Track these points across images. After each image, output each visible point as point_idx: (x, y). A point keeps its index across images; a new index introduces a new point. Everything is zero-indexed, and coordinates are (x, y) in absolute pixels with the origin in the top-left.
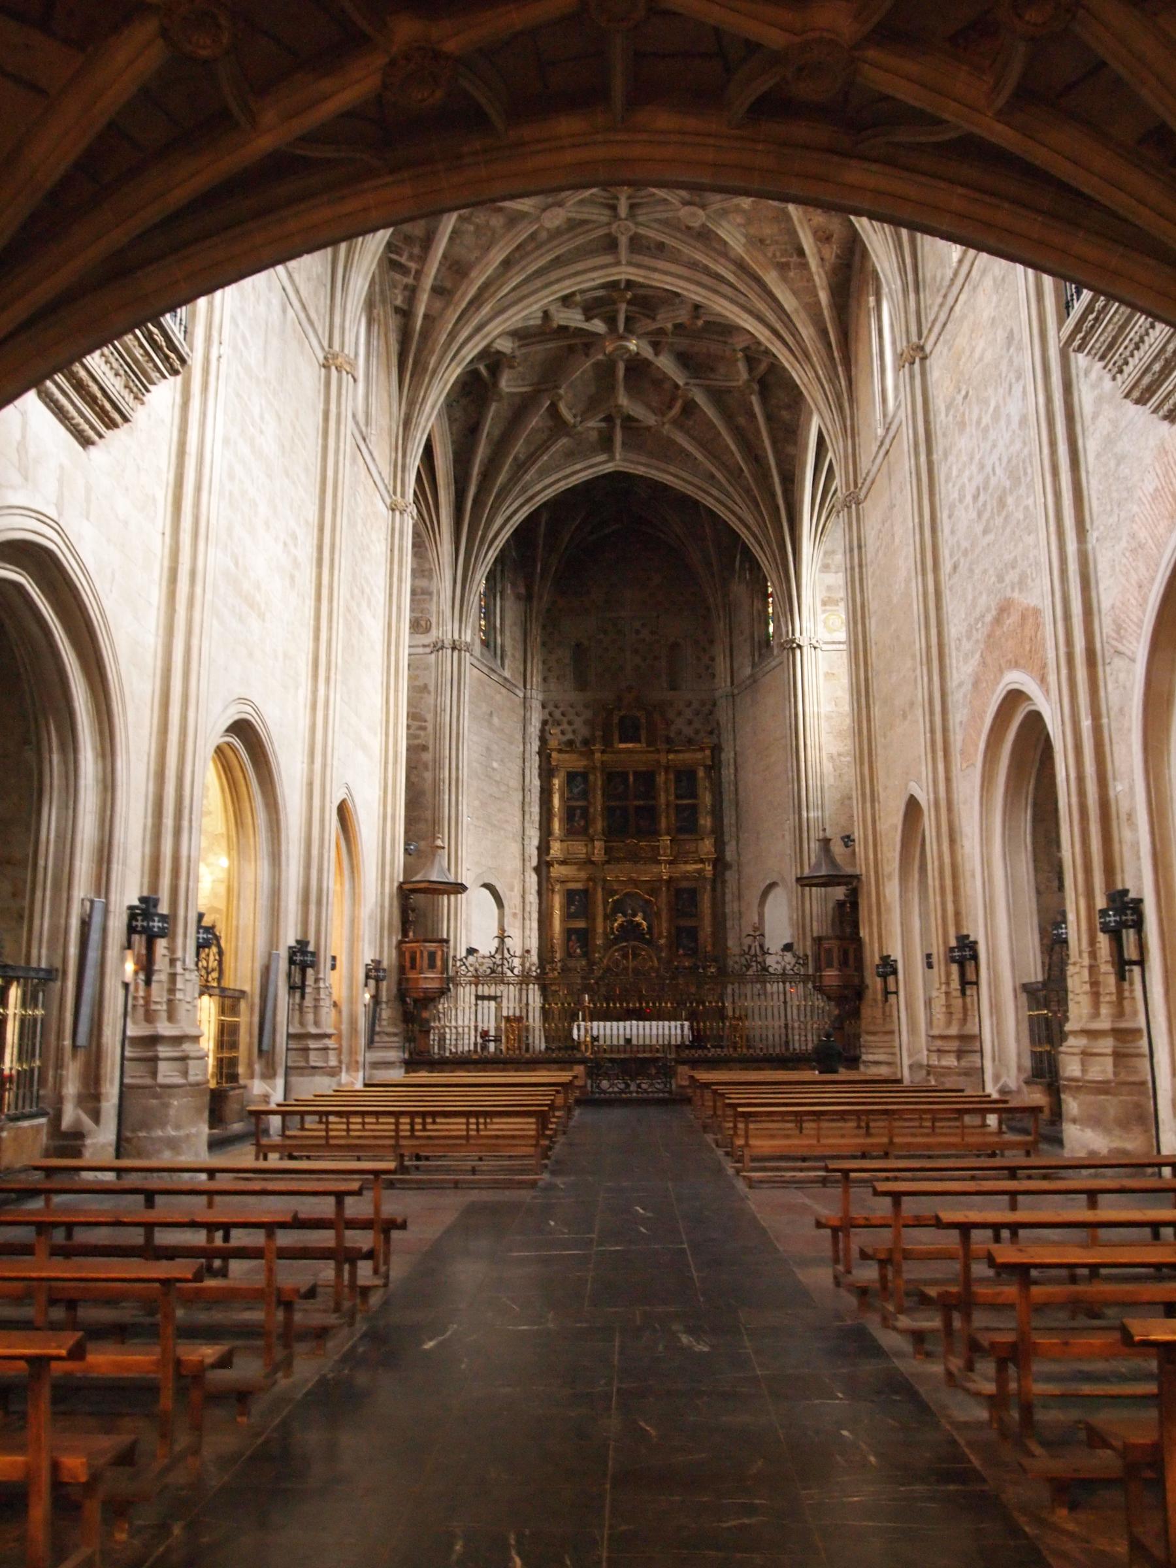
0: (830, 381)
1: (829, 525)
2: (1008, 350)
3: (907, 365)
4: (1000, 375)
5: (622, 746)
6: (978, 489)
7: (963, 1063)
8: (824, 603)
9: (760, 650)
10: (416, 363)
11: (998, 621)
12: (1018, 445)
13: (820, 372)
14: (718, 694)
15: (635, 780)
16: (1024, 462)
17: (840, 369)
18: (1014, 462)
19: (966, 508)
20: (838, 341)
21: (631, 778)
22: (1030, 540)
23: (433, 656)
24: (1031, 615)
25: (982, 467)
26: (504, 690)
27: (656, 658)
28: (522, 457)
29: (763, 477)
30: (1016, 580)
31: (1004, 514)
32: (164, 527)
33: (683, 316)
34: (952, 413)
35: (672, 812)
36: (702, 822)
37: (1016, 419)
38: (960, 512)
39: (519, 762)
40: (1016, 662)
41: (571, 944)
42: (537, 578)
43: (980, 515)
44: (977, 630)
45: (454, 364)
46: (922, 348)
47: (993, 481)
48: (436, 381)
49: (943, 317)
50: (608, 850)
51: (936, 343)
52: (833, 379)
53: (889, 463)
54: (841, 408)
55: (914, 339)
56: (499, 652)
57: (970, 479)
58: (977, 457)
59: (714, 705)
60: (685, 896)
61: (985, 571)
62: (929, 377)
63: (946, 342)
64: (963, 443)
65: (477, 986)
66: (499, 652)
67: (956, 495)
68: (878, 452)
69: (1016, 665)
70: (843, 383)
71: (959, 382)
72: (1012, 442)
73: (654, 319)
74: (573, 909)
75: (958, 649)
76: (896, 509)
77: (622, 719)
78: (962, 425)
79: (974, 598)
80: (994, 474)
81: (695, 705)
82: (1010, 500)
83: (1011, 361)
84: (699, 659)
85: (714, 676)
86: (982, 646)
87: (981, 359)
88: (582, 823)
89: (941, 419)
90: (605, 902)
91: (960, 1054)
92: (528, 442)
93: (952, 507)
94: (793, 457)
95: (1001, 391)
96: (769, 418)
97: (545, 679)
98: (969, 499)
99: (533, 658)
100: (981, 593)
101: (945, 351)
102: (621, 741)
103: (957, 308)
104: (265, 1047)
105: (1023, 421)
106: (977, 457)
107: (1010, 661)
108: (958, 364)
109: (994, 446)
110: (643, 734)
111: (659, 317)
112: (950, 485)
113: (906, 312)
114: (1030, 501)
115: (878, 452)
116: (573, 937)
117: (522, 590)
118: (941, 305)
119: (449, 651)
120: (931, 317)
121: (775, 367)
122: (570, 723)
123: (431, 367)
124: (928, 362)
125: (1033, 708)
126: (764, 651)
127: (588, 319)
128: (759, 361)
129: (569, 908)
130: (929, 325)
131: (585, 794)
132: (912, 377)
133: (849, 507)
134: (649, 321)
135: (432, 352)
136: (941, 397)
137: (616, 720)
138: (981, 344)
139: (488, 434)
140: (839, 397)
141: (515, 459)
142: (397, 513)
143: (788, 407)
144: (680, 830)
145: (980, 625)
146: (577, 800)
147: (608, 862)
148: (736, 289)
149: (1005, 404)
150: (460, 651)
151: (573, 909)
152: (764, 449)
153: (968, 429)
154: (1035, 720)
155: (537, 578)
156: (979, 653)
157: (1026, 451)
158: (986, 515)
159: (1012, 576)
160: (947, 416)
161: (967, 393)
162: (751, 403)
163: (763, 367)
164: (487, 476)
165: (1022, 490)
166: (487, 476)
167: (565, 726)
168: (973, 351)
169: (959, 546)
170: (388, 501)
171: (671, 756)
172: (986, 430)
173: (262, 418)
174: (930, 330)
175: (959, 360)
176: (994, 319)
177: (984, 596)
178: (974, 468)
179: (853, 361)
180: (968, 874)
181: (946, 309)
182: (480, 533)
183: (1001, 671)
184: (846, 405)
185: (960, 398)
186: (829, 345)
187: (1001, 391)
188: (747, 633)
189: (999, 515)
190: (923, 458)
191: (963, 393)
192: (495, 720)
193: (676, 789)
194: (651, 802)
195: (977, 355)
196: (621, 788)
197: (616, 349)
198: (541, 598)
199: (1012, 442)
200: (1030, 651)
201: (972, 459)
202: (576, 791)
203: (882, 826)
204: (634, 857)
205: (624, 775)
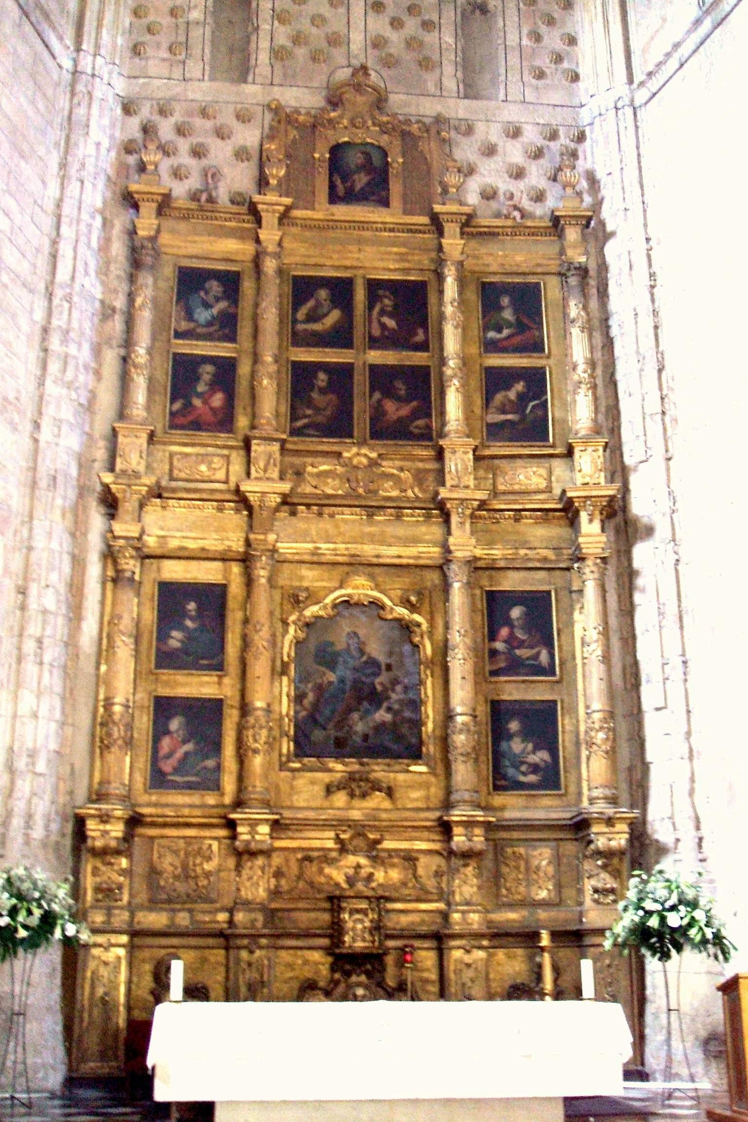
14: (585, 117)
27: (427, 25)
35: (476, 382)
39: (48, 223)
41: (166, 743)
59: (581, 138)
60: (516, 613)
74: (176, 638)
77: (336, 150)
81: (531, 136)
84: (537, 37)
85: (575, 78)
88: (218, 400)
97: (136, 50)
102: (334, 198)
110: (396, 188)
122: (198, 152)
129: (162, 635)
137: (322, 154)
144: (495, 431)
146: (209, 337)
147: (288, 502)
151: (176, 638)
167: (184, 158)
193: (486, 328)
194: (418, 358)
202: (203, 315)
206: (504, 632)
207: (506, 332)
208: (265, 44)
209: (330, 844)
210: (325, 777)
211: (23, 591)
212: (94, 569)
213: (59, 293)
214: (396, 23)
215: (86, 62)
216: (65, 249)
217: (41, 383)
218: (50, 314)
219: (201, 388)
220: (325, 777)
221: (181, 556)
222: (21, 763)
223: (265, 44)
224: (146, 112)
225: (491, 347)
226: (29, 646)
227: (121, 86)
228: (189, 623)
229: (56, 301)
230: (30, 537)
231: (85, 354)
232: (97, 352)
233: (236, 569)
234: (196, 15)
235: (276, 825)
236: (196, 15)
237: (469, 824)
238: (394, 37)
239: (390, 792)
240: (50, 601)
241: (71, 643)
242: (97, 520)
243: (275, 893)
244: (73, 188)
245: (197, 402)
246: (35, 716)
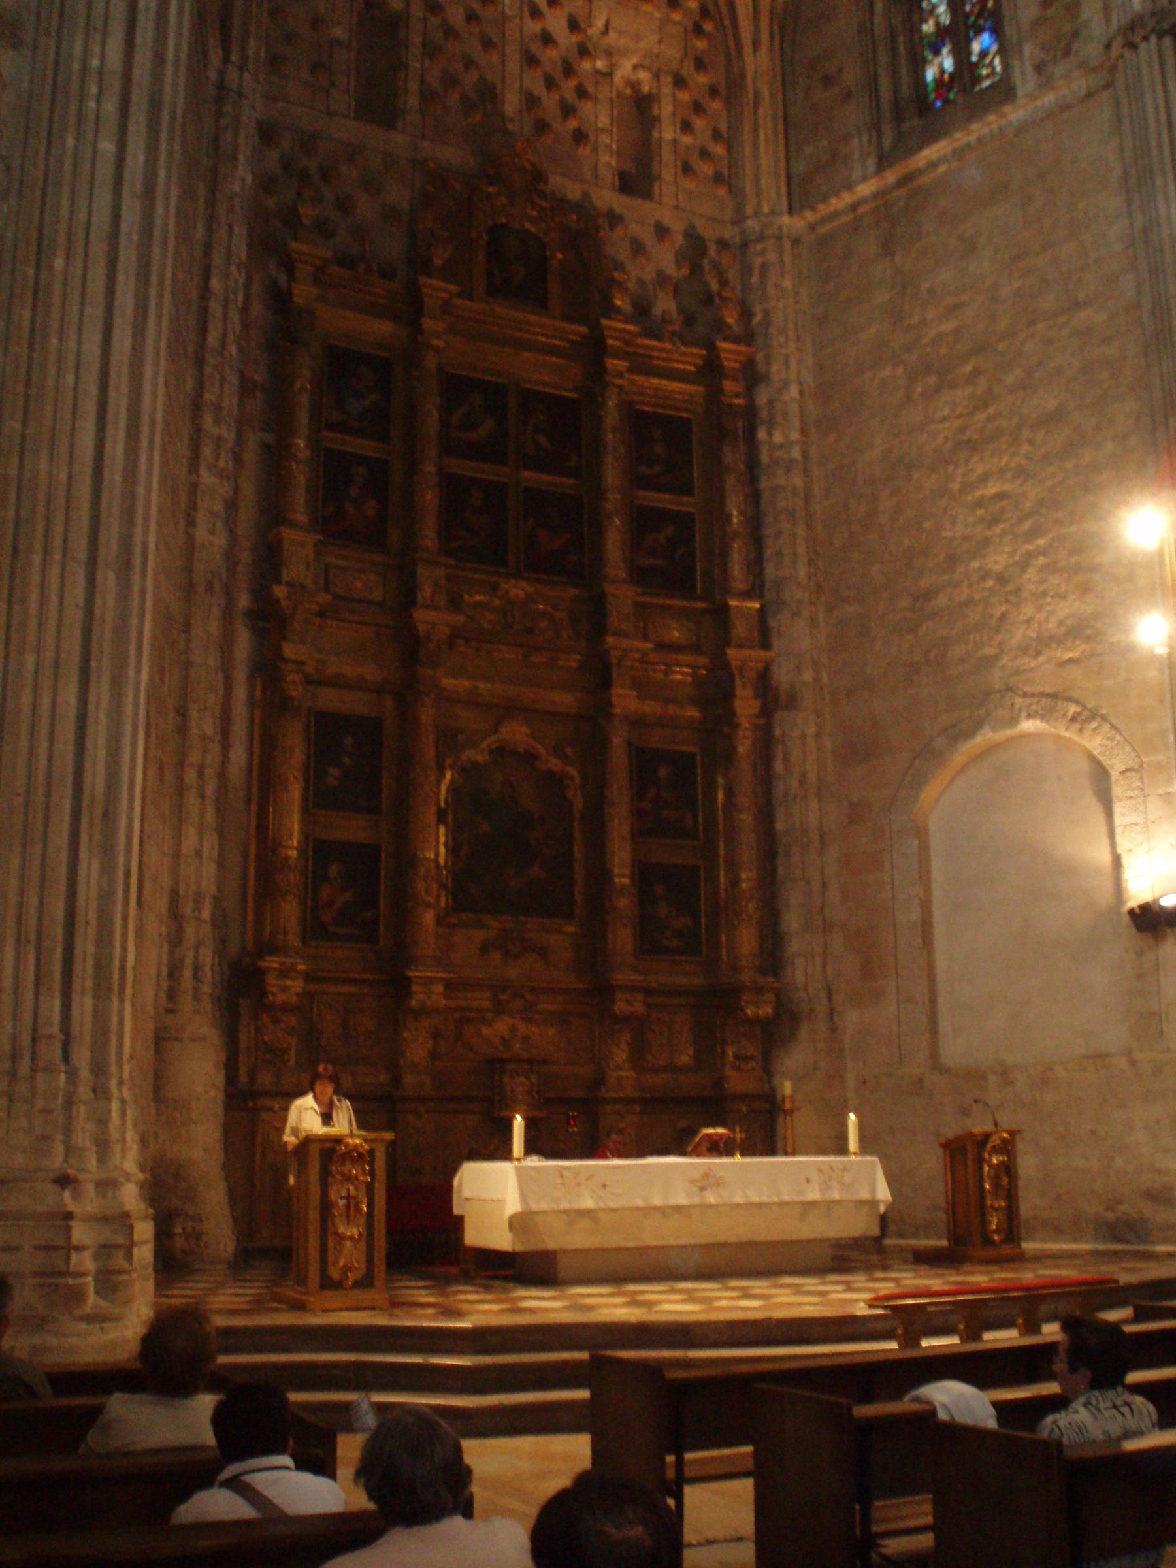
41: (325, 892)
116: (333, 870)
196: (487, 427)
206: (652, 791)
207: (657, 469)
208: (414, 86)
209: (486, 1004)
210: (481, 935)
213: (211, 360)
215: (233, 75)
217: (194, 467)
219: (354, 492)
220: (481, 935)
222: (188, 909)
226: (191, 775)
228: (346, 760)
229: (208, 370)
230: (187, 650)
231: (228, 434)
233: (389, 702)
235: (449, 985)
238: (550, 102)
239: (543, 952)
240: (209, 726)
241: (222, 775)
243: (434, 1055)
244: (221, 233)
245: (351, 509)
246: (199, 854)
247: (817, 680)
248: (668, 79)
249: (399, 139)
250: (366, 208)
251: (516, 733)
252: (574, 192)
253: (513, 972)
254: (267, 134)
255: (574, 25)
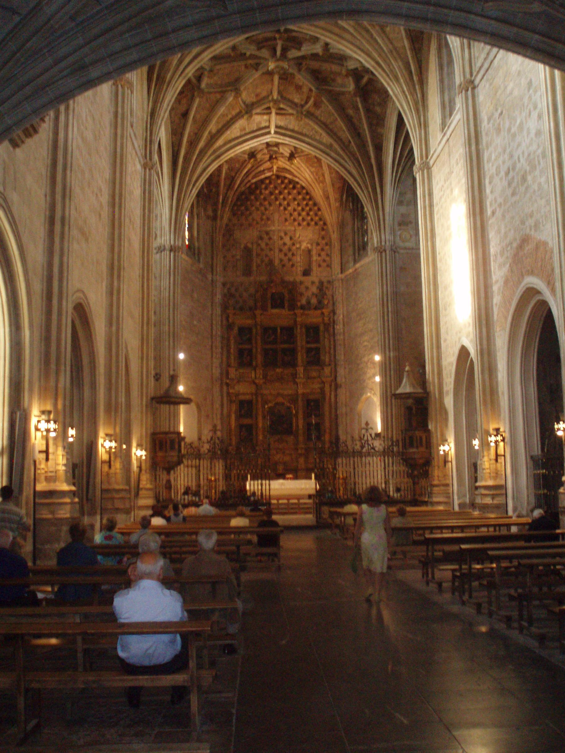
0: (411, 94)
1: (403, 177)
2: (529, 91)
3: (464, 92)
4: (524, 105)
5: (275, 311)
6: (509, 169)
7: (495, 502)
8: (400, 224)
9: (359, 250)
10: (158, 79)
11: (521, 247)
12: (534, 147)
13: (405, 89)
15: (281, 332)
16: (538, 157)
17: (417, 87)
18: (532, 157)
19: (501, 179)
20: (416, 70)
21: (279, 331)
22: (543, 202)
23: (158, 255)
24: (541, 245)
25: (511, 156)
26: (200, 276)
28: (214, 131)
29: (362, 146)
30: (533, 224)
31: (525, 185)
32: (46, 191)
33: (318, 49)
34: (492, 122)
36: (322, 358)
37: (533, 132)
38: (496, 180)
40: (532, 271)
41: (242, 433)
42: (220, 205)
43: (509, 184)
44: (507, 251)
45: (181, 78)
46: (472, 82)
47: (518, 166)
48: (170, 88)
49: (486, 66)
50: (265, 376)
51: (481, 80)
52: (413, 92)
53: (449, 146)
54: (417, 111)
55: (468, 76)
56: (196, 252)
57: (504, 163)
58: (508, 151)
61: (513, 218)
62: (476, 99)
63: (488, 80)
64: (498, 141)
65: (200, 460)
66: (196, 252)
67: (494, 171)
68: (442, 139)
69: (531, 273)
70: (419, 95)
71: (496, 105)
72: (531, 144)
73: (299, 49)
75: (494, 261)
76: (453, 175)
77: (273, 295)
78: (498, 130)
79: (505, 233)
80: (519, 161)
82: (529, 178)
83: (530, 97)
86: (510, 260)
87: (511, 93)
89: (485, 125)
90: (263, 407)
91: (493, 497)
92: (217, 122)
93: (491, 178)
94: (382, 136)
95: (524, 114)
96: (368, 111)
97: (225, 269)
98: (502, 174)
99: (217, 256)
100: (510, 230)
101: (487, 86)
103: (496, 61)
104: (90, 497)
105: (538, 133)
106: (508, 151)
107: (528, 271)
108: (496, 94)
109: (519, 145)
110: (286, 305)
111: (303, 49)
112: (491, 164)
113: (463, 60)
114: (543, 180)
115: (442, 139)
116: (244, 429)
117: (210, 213)
118: (485, 59)
119: (168, 253)
120: (479, 64)
121: (373, 80)
123: (167, 80)
124: (476, 91)
125: (541, 298)
126: (361, 252)
127: (259, 49)
128: (363, 77)
129: (240, 411)
130: (477, 69)
131: (249, 341)
132: (467, 98)
133: (423, 171)
134: (296, 51)
135: (168, 71)
136: (484, 112)
137: (269, 295)
138: (511, 85)
139: (194, 117)
140: (416, 103)
141: (210, 133)
142: (147, 170)
143: (380, 104)
145: (509, 248)
147: (265, 383)
148: (355, 37)
149: (526, 122)
150: (175, 252)
152: (364, 130)
153: (502, 133)
154: (544, 304)
155: (220, 205)
156: (508, 266)
157: (540, 151)
158: (514, 185)
159: (531, 222)
160: (488, 123)
161: (502, 113)
162: (357, 102)
163: (365, 80)
164: (192, 144)
165: (537, 173)
166: (192, 144)
168: (506, 88)
169: (496, 201)
170: (142, 163)
171: (304, 317)
172: (514, 135)
173: (86, 120)
174: (478, 72)
175: (496, 92)
176: (519, 72)
177: (512, 231)
178: (506, 157)
179: (425, 82)
180: (500, 393)
181: (489, 61)
182: (187, 178)
183: (522, 276)
184: (421, 109)
185: (497, 115)
186: (411, 72)
187: (524, 114)
188: (351, 241)
189: (522, 185)
190: (473, 147)
191: (499, 111)
192: (195, 295)
194: (292, 346)
195: (508, 92)
197: (277, 67)
198: (222, 218)
199: (531, 144)
200: (541, 266)
201: (504, 151)
203: (444, 363)
204: (280, 379)
205: (274, 330)
208: (255, 264)
211: (212, 404)
212: (225, 399)
213: (214, 338)
214: (286, 255)
215: (215, 278)
216: (214, 327)
218: (212, 342)
219: (245, 356)
221: (244, 394)
223: (255, 264)
224: (228, 286)
225: (308, 342)
227: (222, 280)
232: (222, 348)
233: (254, 397)
234: (238, 257)
236: (238, 257)
237: (302, 448)
238: (285, 259)
242: (225, 388)
247: (346, 381)
248: (314, 245)
249: (252, 278)
250: (245, 294)
251: (280, 400)
252: (292, 279)
253: (280, 446)
254: (224, 284)
255: (291, 238)
